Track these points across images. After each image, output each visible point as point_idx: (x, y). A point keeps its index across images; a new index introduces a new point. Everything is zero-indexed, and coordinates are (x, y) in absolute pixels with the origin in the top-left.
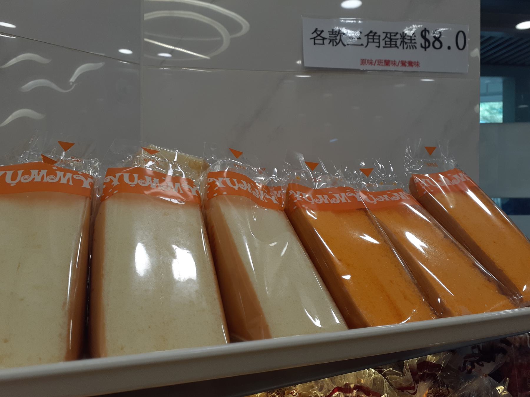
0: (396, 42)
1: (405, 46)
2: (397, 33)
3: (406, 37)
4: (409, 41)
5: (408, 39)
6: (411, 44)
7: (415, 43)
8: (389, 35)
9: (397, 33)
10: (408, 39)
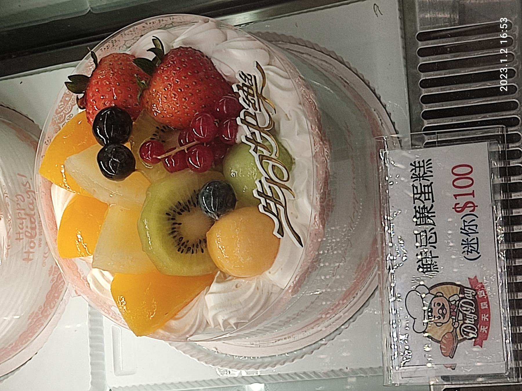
0: (424, 186)
1: (429, 174)
2: (413, 186)
3: (417, 173)
4: (422, 169)
5: (420, 171)
6: (426, 167)
7: (423, 161)
8: (418, 196)
9: (413, 186)
10: (420, 171)
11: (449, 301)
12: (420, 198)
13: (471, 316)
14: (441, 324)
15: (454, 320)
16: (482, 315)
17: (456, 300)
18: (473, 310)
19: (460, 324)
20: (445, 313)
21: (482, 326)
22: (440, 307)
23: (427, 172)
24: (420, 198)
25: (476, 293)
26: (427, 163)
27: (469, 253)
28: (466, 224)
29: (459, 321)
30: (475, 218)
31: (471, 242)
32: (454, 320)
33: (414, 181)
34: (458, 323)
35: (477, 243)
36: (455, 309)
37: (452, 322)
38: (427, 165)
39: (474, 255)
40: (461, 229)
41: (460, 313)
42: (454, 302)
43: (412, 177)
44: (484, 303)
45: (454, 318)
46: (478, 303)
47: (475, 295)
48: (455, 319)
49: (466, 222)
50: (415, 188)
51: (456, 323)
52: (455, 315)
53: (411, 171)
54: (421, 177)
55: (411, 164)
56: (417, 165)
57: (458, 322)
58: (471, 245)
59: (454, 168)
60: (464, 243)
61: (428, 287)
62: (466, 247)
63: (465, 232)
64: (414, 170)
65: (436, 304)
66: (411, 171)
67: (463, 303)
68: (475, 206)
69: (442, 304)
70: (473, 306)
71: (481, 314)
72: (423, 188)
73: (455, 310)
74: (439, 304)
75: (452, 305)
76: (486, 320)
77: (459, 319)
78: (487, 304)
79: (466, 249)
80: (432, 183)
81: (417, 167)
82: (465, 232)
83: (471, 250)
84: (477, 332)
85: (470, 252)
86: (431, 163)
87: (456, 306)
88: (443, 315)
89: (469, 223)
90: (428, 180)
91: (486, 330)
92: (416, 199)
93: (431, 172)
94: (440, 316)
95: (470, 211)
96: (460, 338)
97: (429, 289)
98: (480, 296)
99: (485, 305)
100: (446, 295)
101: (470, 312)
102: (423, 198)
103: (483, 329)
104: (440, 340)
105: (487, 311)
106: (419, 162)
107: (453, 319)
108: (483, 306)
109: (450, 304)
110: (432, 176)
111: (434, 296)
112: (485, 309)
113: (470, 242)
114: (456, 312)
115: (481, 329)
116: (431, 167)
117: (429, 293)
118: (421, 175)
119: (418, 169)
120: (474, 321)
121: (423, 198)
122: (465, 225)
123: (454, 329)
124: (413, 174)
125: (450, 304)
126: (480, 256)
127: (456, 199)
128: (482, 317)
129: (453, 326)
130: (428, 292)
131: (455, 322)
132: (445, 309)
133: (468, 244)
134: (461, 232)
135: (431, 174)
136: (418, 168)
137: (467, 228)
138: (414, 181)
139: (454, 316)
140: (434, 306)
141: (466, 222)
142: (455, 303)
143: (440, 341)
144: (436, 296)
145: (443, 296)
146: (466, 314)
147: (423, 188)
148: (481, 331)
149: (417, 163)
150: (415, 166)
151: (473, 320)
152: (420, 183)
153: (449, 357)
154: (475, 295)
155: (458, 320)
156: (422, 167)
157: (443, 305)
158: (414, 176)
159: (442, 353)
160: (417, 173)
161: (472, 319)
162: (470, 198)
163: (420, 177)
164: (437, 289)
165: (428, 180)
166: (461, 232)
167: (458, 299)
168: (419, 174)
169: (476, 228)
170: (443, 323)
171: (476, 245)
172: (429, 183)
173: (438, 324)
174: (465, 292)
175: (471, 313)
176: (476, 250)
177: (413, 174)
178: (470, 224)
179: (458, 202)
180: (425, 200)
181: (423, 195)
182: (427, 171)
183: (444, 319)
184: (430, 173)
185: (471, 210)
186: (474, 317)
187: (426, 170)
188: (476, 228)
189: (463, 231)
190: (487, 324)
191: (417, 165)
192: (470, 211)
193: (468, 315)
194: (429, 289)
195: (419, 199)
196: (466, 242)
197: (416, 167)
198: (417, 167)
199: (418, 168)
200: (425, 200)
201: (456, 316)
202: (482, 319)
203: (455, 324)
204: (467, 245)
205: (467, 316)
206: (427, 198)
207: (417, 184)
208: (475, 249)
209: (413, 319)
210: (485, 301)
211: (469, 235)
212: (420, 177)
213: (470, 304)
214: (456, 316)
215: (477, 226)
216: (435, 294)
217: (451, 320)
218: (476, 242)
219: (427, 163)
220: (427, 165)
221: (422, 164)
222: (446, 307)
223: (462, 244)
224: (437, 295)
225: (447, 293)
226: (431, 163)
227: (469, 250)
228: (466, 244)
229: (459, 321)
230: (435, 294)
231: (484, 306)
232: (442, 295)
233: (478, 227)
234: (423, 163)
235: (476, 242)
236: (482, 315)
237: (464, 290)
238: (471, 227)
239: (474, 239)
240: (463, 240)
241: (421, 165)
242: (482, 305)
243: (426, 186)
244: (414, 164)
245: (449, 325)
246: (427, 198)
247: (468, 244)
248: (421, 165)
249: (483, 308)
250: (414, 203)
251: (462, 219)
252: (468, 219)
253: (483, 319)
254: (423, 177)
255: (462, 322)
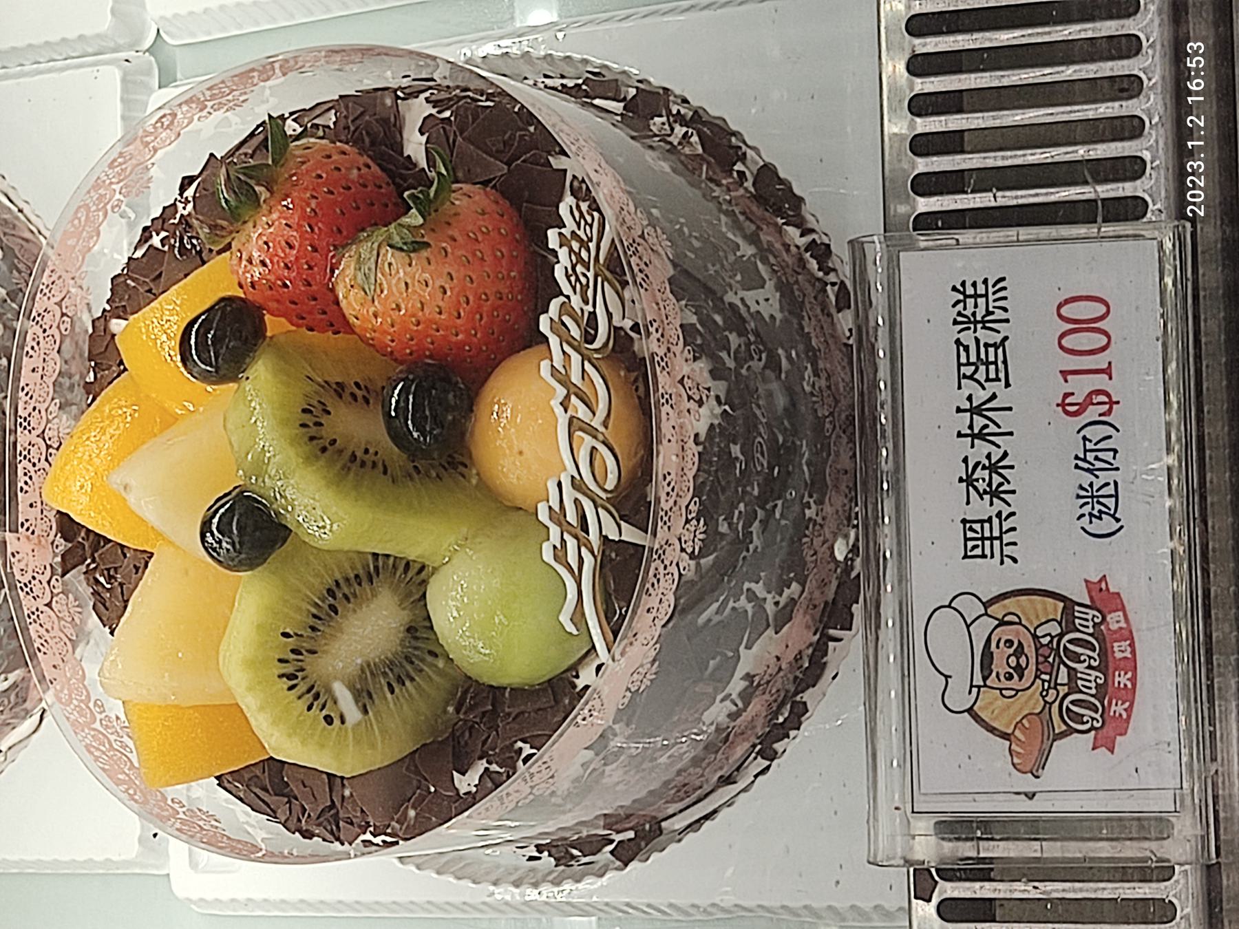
0: (987, 345)
1: (999, 314)
2: (958, 342)
3: (968, 312)
4: (981, 301)
5: (976, 306)
6: (991, 298)
8: (968, 370)
9: (958, 342)
10: (976, 306)
11: (1035, 637)
12: (976, 376)
13: (1089, 675)
14: (1013, 693)
15: (1046, 685)
16: (1117, 673)
17: (1053, 634)
18: (1095, 660)
19: (1061, 695)
20: (1024, 666)
21: (1114, 702)
22: (1011, 651)
23: (996, 310)
24: (976, 376)
25: (1104, 618)
26: (994, 286)
27: (1093, 519)
28: (1089, 446)
29: (1058, 687)
30: (1111, 431)
31: (1100, 493)
32: (1046, 685)
33: (959, 332)
34: (1055, 692)
35: (1116, 496)
36: (1049, 656)
37: (1041, 689)
38: (994, 293)
39: (1107, 524)
40: (1077, 458)
41: (1062, 666)
42: (1048, 638)
43: (955, 320)
44: (1123, 643)
45: (1047, 677)
46: (1109, 645)
47: (1101, 623)
48: (1049, 682)
49: (1090, 441)
50: (961, 348)
51: (1051, 691)
52: (1049, 670)
53: (954, 306)
54: (979, 322)
55: (954, 289)
56: (970, 291)
57: (1055, 688)
58: (1101, 500)
59: (1067, 302)
60: (1083, 493)
61: (984, 600)
62: (1088, 503)
63: (1086, 466)
64: (962, 304)
65: (1002, 644)
66: (954, 306)
67: (1070, 641)
68: (1112, 403)
69: (1016, 645)
70: (1094, 650)
71: (1116, 670)
72: (982, 350)
73: (1051, 660)
74: (1009, 643)
75: (1042, 646)
76: (1125, 685)
77: (1059, 681)
78: (1130, 645)
79: (1087, 509)
80: (1006, 338)
81: (970, 296)
82: (1086, 466)
83: (1100, 511)
84: (1102, 716)
85: (1095, 517)
86: (1004, 288)
87: (1052, 649)
88: (1020, 670)
89: (1096, 444)
90: (998, 332)
91: (1125, 710)
92: (965, 377)
93: (1005, 310)
94: (1011, 671)
95: (1100, 415)
96: (1059, 727)
97: (986, 605)
98: (1114, 627)
99: (1123, 648)
100: (1028, 619)
101: (1086, 664)
102: (981, 376)
103: (1118, 708)
104: (1010, 731)
105: (1131, 664)
106: (974, 285)
107: (1044, 681)
108: (1120, 650)
109: (1038, 645)
110: (1007, 321)
111: (997, 622)
112: (1125, 658)
113: (1097, 491)
114: (1052, 666)
115: (1113, 708)
116: (1005, 298)
117: (986, 614)
118: (979, 318)
119: (970, 302)
120: (1096, 688)
121: (981, 376)
122: (1087, 448)
123: (1045, 706)
124: (959, 314)
125: (1038, 645)
126: (1122, 527)
127: (1066, 381)
128: (1117, 679)
129: (1043, 697)
130: (983, 612)
131: (1049, 687)
132: (1024, 657)
133: (1092, 497)
134: (1077, 467)
135: (1003, 315)
136: (973, 300)
137: (1090, 456)
138: (959, 332)
139: (1046, 674)
140: (998, 647)
141: (1090, 441)
142: (1051, 642)
143: (1008, 734)
144: (1002, 623)
145: (1020, 623)
146: (1074, 669)
147: (982, 350)
148: (1112, 714)
149: (968, 285)
150: (964, 293)
151: (1093, 685)
152: (976, 338)
153: (1030, 775)
154: (1101, 623)
155: (1056, 684)
156: (981, 296)
157: (1020, 643)
158: (960, 319)
159: (1013, 764)
160: (968, 312)
161: (1090, 681)
162: (1100, 381)
163: (976, 322)
164: (1005, 606)
165: (998, 332)
166: (1077, 467)
167: (1059, 631)
168: (974, 314)
169: (1114, 458)
170: (1018, 691)
171: (1113, 499)
172: (998, 338)
173: (1004, 692)
174: (1076, 614)
175: (1090, 667)
176: (1112, 512)
177: (959, 314)
178: (1098, 447)
179: (1070, 391)
180: (988, 380)
181: (982, 368)
182: (994, 307)
183: (1020, 679)
184: (1001, 311)
185: (1102, 411)
186: (1097, 677)
187: (991, 304)
188: (1114, 458)
189: (1081, 464)
190: (1129, 694)
191: (970, 291)
192: (1100, 415)
193: (1082, 673)
194: (986, 605)
195: (971, 377)
196: (1087, 491)
197: (966, 296)
198: (970, 296)
199: (973, 300)
200: (986, 381)
201: (1051, 675)
202: (1116, 685)
203: (1047, 695)
204: (1090, 500)
205: (1079, 675)
206: (992, 375)
207: (968, 338)
208: (1109, 509)
209: (943, 678)
210: (1125, 641)
211: (1096, 473)
212: (976, 322)
213: (1090, 646)
214: (1051, 675)
215: (1115, 451)
216: (1000, 617)
217: (1038, 682)
218: (1113, 492)
219: (994, 286)
220: (994, 293)
221: (981, 289)
222: (1026, 650)
223: (1079, 497)
224: (1006, 619)
225: (1033, 617)
226: (1004, 288)
227: (1095, 512)
228: (1088, 495)
229: (1058, 687)
230: (1000, 617)
231: (1123, 651)
232: (1017, 620)
233: (1117, 455)
234: (984, 286)
235: (1113, 492)
236: (1117, 673)
237: (1074, 611)
238: (1100, 455)
239: (1107, 484)
240: (1081, 488)
241: (979, 292)
242: (1116, 649)
243: (991, 346)
244: (962, 289)
245: (1033, 694)
246: (992, 375)
247: (1092, 497)
248: (979, 292)
249: (1118, 655)
250: (960, 387)
251: (1079, 432)
252: (1095, 433)
253: (1119, 683)
254: (983, 322)
255: (1066, 688)
